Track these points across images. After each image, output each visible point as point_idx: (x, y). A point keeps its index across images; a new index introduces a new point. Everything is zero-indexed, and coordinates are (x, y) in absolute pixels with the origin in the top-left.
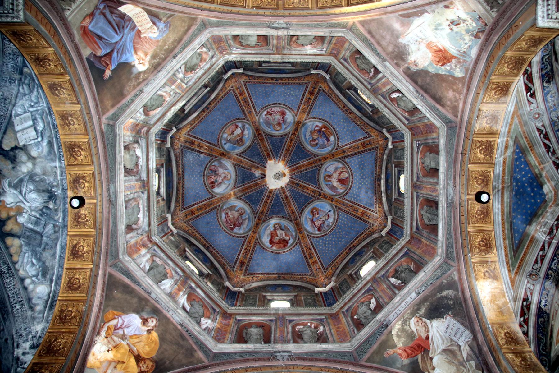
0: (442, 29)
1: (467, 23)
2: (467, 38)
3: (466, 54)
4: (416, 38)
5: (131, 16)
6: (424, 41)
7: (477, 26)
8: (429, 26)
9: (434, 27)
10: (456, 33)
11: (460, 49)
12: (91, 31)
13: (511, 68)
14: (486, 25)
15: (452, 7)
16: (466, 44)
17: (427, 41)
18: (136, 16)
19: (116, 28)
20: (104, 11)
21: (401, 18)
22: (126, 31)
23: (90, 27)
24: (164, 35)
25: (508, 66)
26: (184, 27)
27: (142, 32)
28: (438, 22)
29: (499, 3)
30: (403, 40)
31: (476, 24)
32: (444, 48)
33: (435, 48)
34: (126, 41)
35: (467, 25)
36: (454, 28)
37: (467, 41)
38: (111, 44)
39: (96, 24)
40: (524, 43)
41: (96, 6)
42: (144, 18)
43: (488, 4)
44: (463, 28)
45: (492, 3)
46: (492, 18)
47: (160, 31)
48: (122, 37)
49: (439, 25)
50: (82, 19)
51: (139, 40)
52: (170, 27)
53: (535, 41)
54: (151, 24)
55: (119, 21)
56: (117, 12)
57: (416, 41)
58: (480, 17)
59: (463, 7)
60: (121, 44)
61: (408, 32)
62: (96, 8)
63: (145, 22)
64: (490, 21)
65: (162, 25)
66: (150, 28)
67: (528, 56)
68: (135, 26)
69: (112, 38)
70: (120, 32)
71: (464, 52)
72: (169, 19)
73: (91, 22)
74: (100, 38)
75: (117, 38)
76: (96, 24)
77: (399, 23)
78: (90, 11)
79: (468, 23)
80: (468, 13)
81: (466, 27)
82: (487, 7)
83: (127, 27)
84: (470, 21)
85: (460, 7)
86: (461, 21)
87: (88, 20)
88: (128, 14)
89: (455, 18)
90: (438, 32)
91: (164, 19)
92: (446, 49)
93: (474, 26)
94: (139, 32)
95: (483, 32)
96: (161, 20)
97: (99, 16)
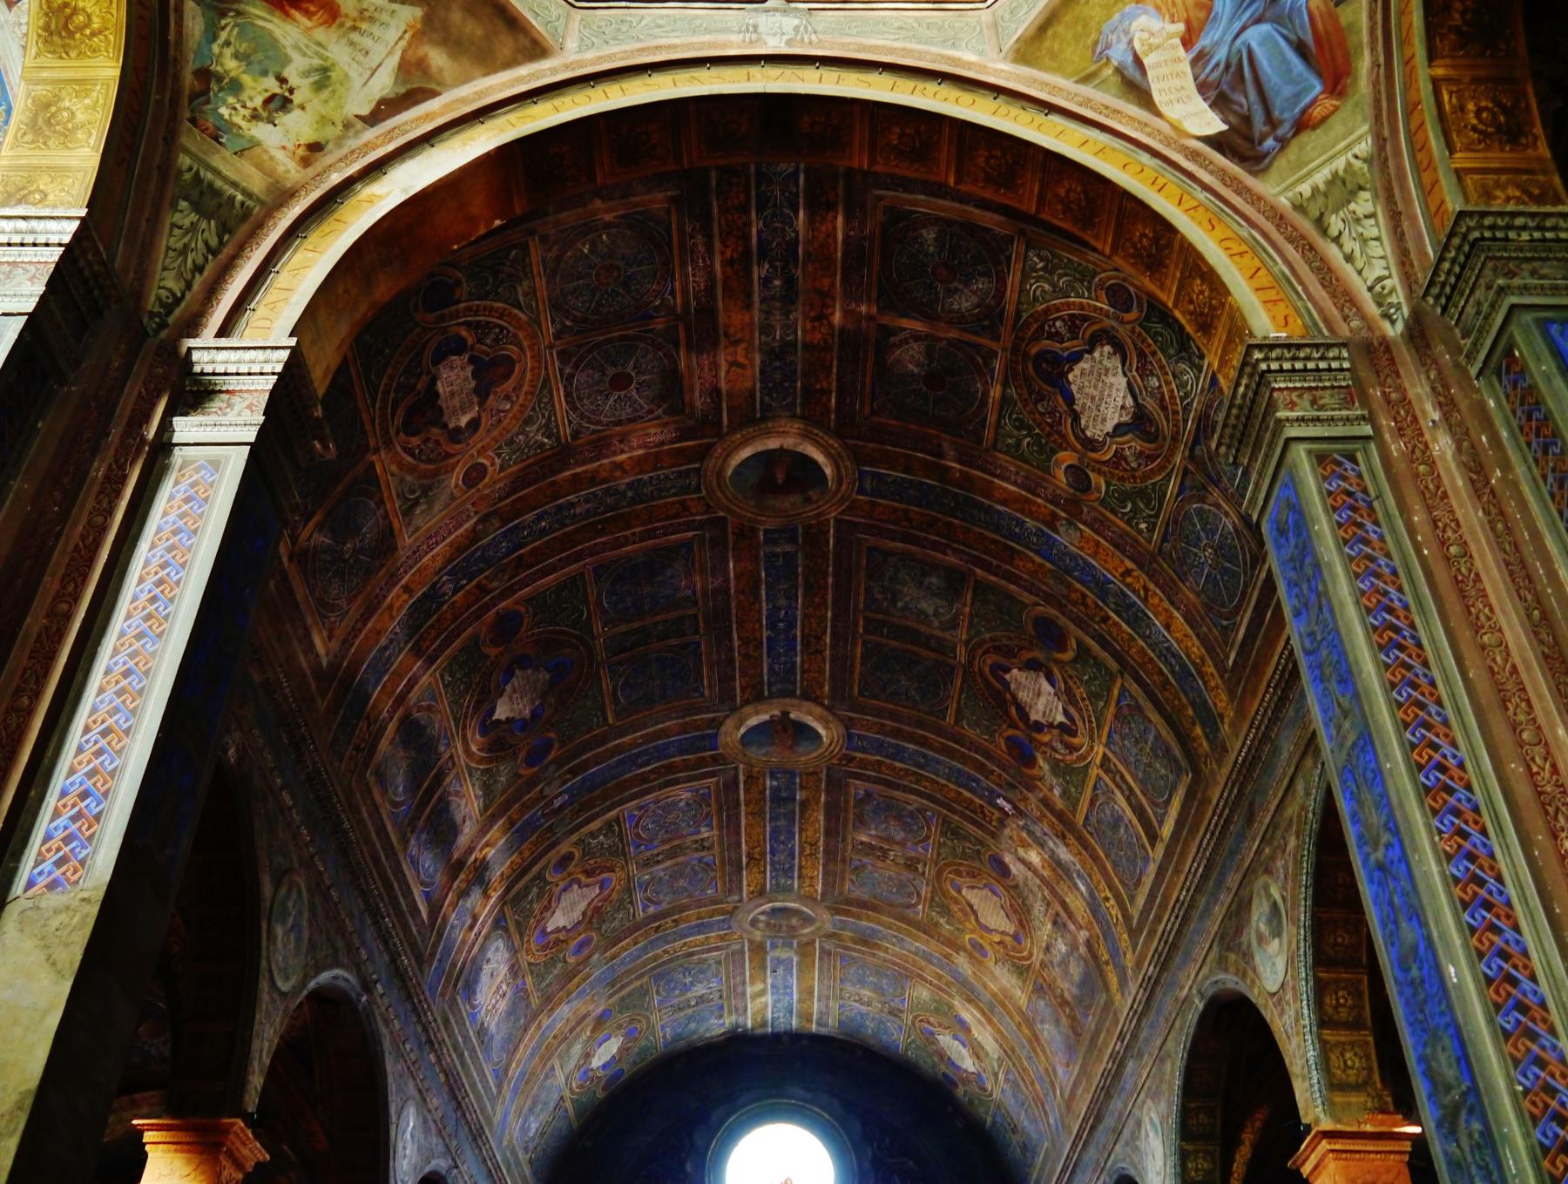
0: (306, 74)
1: (247, 113)
2: (231, 65)
3: (215, 8)
4: (376, 30)
5: (1199, 98)
6: (349, 24)
7: (216, 110)
8: (347, 75)
9: (333, 74)
10: (265, 73)
11: (239, 21)
12: (1320, 75)
13: (75, 11)
14: (193, 121)
15: (301, 152)
16: (227, 43)
17: (342, 25)
18: (1183, 93)
19: (1245, 62)
20: (1266, 129)
21: (433, 86)
22: (1221, 55)
23: (1318, 88)
24: (1117, 16)
25: (89, 16)
26: (1055, 36)
27: (1177, 41)
28: (325, 94)
29: (185, 199)
30: (411, 14)
31: (221, 116)
32: (287, 14)
33: (312, 9)
34: (1234, 16)
35: (244, 107)
36: (275, 87)
37: (228, 52)
38: (1277, 20)
39: (1297, 96)
40: (80, 117)
41: (1282, 148)
42: (1162, 85)
43: (211, 185)
44: (253, 93)
45: (202, 193)
46: (187, 151)
47: (1126, 32)
48: (1237, 36)
49: (319, 86)
50: (1330, 121)
51: (1192, 14)
52: (1096, 43)
53: (48, 122)
54: (1146, 61)
55: (1233, 89)
56: (1231, 118)
57: (372, 19)
58: (216, 139)
59: (272, 158)
60: (1248, 14)
61: (403, 43)
62: (1284, 143)
63: (1164, 70)
64: (190, 139)
65: (1119, 54)
66: (1152, 48)
67: (43, 61)
68: (1194, 62)
69: (1265, 40)
70: (1240, 52)
71: (223, 14)
72: (1093, 68)
73: (1314, 101)
74: (1300, 49)
75: (1254, 35)
76: (1297, 96)
77: (434, 70)
78: (1305, 137)
79: (243, 111)
80: (255, 144)
81: (244, 96)
82: (210, 176)
83: (1217, 65)
84: (238, 120)
85: (280, 155)
86: (265, 114)
87: (1317, 112)
88: (1205, 106)
89: (285, 119)
90: (317, 62)
91: (1108, 71)
92: (278, 13)
93: (227, 110)
94: (1187, 42)
95: (194, 96)
96: (1119, 71)
97: (1286, 115)
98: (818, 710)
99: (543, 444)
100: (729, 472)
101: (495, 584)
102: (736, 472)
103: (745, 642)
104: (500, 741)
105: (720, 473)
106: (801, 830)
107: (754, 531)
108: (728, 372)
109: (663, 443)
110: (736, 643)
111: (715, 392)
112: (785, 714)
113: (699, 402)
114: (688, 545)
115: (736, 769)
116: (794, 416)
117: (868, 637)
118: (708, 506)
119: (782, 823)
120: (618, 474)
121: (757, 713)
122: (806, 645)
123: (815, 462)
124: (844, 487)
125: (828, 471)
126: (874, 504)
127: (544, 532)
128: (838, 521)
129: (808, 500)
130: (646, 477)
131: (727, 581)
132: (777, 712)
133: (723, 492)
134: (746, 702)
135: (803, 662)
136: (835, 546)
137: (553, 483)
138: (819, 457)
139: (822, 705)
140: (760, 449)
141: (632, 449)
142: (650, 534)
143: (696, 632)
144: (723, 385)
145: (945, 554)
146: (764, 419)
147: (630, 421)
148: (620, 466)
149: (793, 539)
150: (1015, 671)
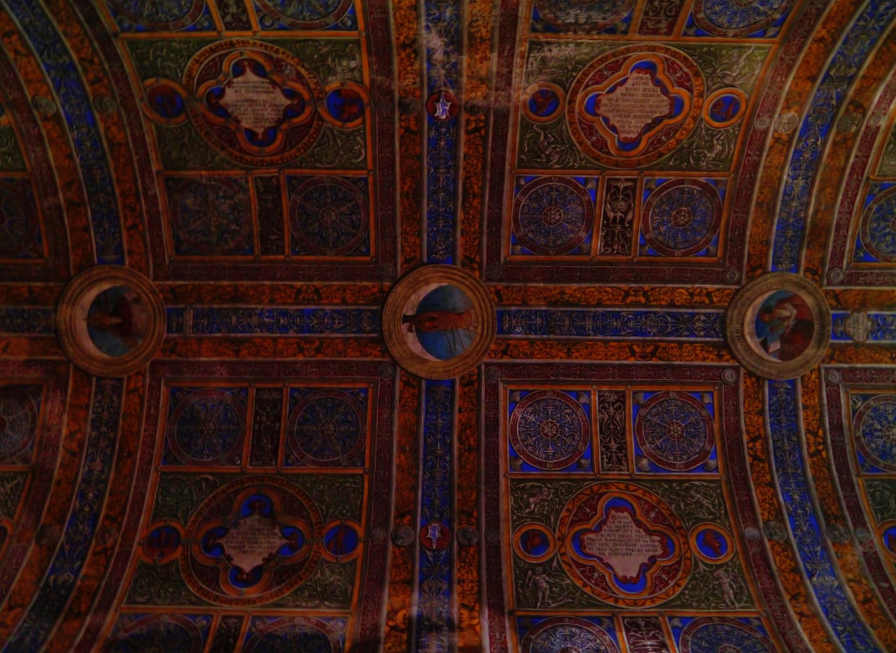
98: (400, 289)
99: (17, 485)
100: (106, 356)
101: (110, 542)
102: (108, 352)
103: (301, 351)
104: (280, 573)
105: (106, 363)
106: (600, 304)
107: (168, 341)
108: (12, 354)
109: (63, 402)
110: (301, 358)
111: (28, 364)
112: (406, 319)
113: (33, 375)
114: (173, 391)
115: (487, 365)
116: (55, 311)
117: (257, 251)
118: (139, 373)
119: (589, 324)
120: (79, 436)
121: (404, 343)
122: (309, 302)
123: (98, 296)
124: (120, 275)
125: (105, 286)
126: (130, 253)
127: (99, 497)
128: (156, 278)
129: (138, 300)
130: (91, 416)
131: (222, 363)
132: (405, 327)
133: (127, 362)
134: (385, 352)
135: (330, 304)
136: (185, 279)
137: (58, 483)
138: (93, 293)
139: (391, 288)
140: (86, 334)
141: (60, 423)
142: (152, 420)
143: (280, 390)
144: (23, 357)
145: (155, 196)
146: (56, 331)
147: (34, 421)
148: (71, 435)
149: (180, 313)
150: (245, 124)
